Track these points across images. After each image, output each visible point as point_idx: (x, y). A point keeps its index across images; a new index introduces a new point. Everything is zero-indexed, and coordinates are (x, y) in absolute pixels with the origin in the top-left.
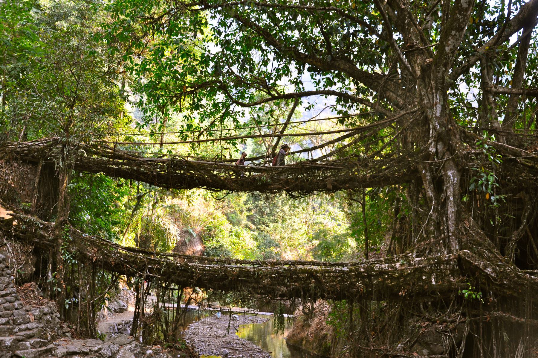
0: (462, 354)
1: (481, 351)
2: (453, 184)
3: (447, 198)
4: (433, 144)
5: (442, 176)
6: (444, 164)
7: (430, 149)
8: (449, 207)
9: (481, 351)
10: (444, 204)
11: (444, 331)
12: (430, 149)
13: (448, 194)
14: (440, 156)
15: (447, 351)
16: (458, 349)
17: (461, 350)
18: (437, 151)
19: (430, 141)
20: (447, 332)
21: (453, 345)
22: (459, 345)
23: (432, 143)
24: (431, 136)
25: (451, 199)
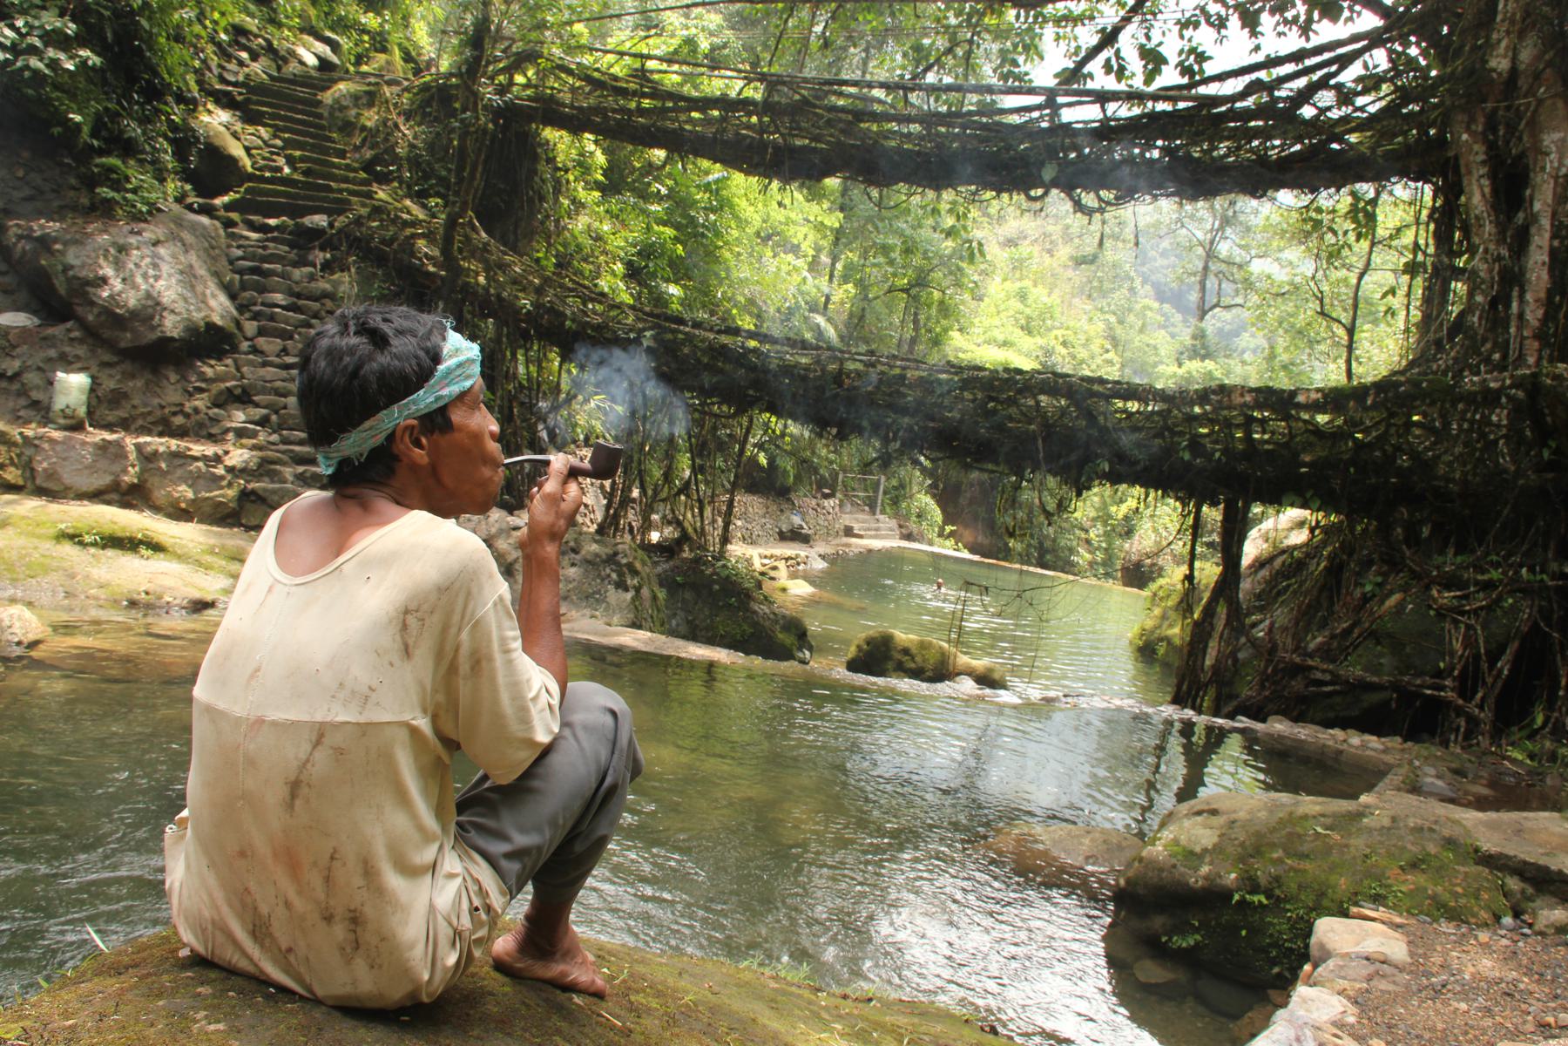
0: (1500, 684)
1: (1563, 682)
2: (1556, 178)
3: (1533, 218)
4: (1503, 44)
5: (1522, 155)
6: (1535, 111)
7: (1493, 63)
8: (1532, 248)
9: (1563, 682)
10: (1520, 242)
11: (1452, 610)
12: (1493, 63)
13: (1537, 206)
14: (1523, 83)
15: (1453, 669)
16: (1490, 669)
17: (1500, 671)
18: (1514, 72)
19: (1495, 36)
20: (1463, 613)
21: (1477, 657)
22: (1493, 657)
23: (1499, 41)
24: (1499, 18)
25: (1546, 222)
